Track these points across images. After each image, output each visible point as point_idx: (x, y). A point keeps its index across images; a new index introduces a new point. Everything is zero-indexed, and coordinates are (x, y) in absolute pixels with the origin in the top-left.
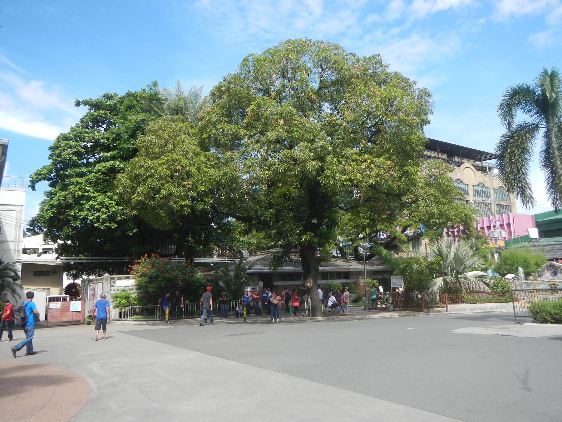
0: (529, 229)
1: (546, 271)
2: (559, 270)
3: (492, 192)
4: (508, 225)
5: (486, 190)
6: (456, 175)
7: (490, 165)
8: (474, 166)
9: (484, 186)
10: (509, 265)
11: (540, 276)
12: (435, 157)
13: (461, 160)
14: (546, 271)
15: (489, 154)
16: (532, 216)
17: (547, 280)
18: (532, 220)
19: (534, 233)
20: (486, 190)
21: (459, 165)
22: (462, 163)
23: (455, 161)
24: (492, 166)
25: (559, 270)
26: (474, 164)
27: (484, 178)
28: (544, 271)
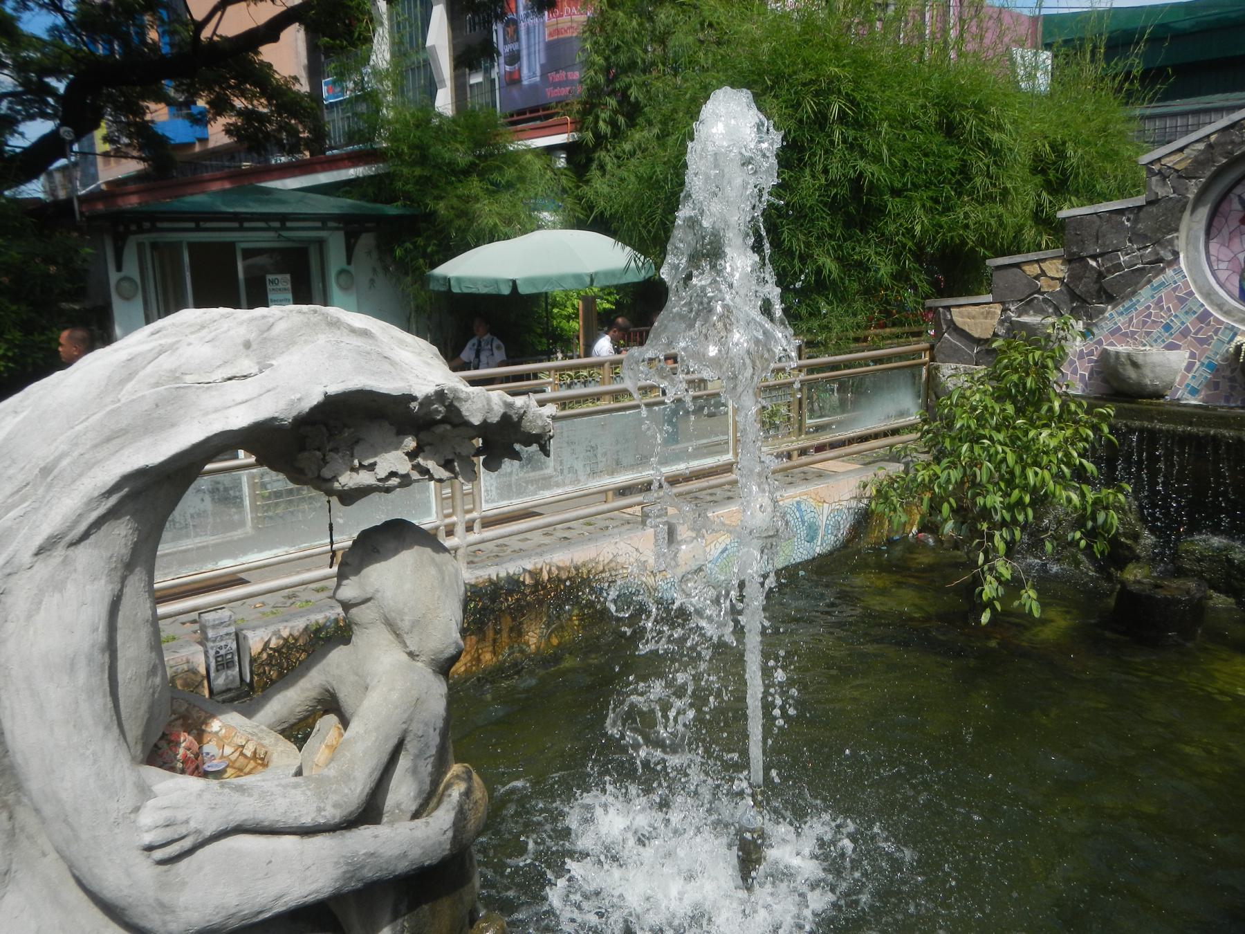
1: (1193, 224)
11: (1092, 293)
14: (1193, 224)
28: (1156, 225)
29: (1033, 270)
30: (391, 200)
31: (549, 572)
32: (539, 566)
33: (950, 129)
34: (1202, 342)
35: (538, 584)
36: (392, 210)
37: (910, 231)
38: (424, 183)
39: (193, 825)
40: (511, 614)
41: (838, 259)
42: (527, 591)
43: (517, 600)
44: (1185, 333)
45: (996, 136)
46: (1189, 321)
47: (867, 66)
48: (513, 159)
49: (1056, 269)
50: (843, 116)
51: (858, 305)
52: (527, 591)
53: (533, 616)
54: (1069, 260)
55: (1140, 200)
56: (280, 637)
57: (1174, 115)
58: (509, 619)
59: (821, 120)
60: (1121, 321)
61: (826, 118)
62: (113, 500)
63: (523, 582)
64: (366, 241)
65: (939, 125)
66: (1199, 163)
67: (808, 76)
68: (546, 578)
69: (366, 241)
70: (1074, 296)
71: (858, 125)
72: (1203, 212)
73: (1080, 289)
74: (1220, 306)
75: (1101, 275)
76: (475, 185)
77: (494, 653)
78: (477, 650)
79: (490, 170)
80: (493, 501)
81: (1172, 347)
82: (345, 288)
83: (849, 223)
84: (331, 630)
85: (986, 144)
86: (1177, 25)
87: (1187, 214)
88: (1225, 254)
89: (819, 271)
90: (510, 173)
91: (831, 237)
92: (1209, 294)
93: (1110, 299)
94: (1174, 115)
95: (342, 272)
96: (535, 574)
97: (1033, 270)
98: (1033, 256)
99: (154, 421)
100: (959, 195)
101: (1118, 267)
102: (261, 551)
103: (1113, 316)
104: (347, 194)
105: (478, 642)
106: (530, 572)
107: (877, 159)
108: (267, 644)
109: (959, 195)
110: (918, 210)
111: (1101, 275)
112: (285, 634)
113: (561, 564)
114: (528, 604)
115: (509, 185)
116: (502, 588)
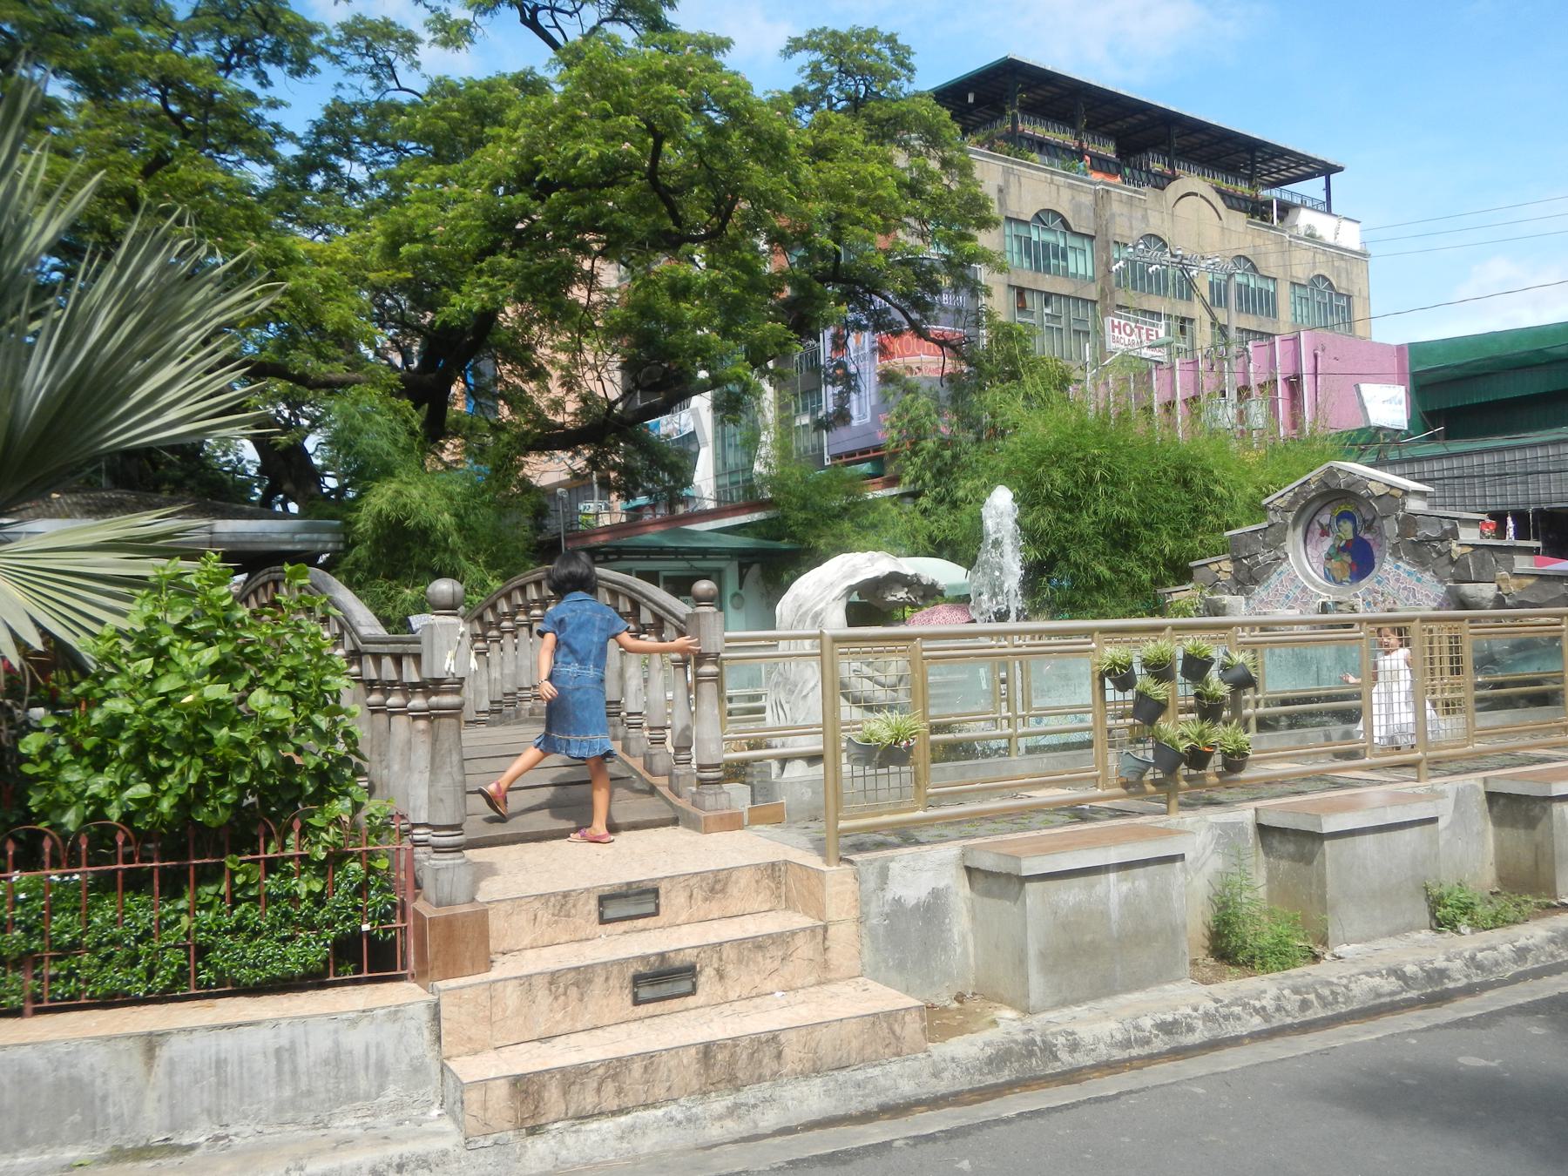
0: (1363, 387)
1: (1294, 539)
2: (1391, 528)
3: (1284, 296)
4: (1294, 384)
5: (1262, 284)
6: (1145, 218)
7: (1286, 197)
8: (1219, 191)
9: (1254, 268)
10: (1049, 500)
11: (1246, 580)
12: (1066, 149)
13: (1171, 166)
14: (1294, 539)
15: (1282, 153)
16: (1400, 348)
17: (1293, 614)
18: (1401, 364)
19: (1388, 406)
20: (1262, 284)
21: (1161, 182)
22: (1173, 178)
23: (1149, 171)
24: (1297, 200)
25: (1391, 528)
26: (1224, 186)
27: (1259, 241)
28: (1274, 538)
29: (1214, 567)
30: (779, 539)
33: (1186, 484)
34: (1306, 603)
36: (784, 544)
37: (1161, 551)
38: (809, 524)
41: (1111, 568)
44: (1296, 599)
45: (1218, 489)
46: (1297, 592)
47: (1118, 448)
48: (873, 505)
49: (1227, 566)
50: (1103, 478)
51: (1128, 600)
54: (1235, 560)
55: (1265, 525)
57: (1533, 446)
59: (1090, 480)
60: (1264, 594)
61: (1092, 478)
64: (755, 570)
65: (1177, 481)
66: (1292, 503)
67: (1080, 455)
69: (755, 570)
70: (1238, 582)
71: (1115, 485)
72: (1300, 530)
73: (1240, 577)
74: (1313, 583)
75: (1250, 569)
76: (847, 526)
79: (858, 515)
81: (1291, 608)
82: (737, 608)
83: (1115, 544)
85: (1209, 493)
86: (1555, 351)
87: (1290, 532)
88: (1315, 554)
89: (1098, 578)
90: (873, 517)
91: (1104, 554)
92: (1307, 577)
93: (1257, 582)
94: (1533, 446)
95: (735, 595)
97: (1214, 567)
98: (1214, 559)
99: (852, 575)
100: (1195, 528)
101: (1258, 563)
103: (1260, 591)
104: (745, 534)
107: (1129, 504)
109: (1195, 528)
110: (1164, 537)
111: (1250, 569)
115: (874, 526)
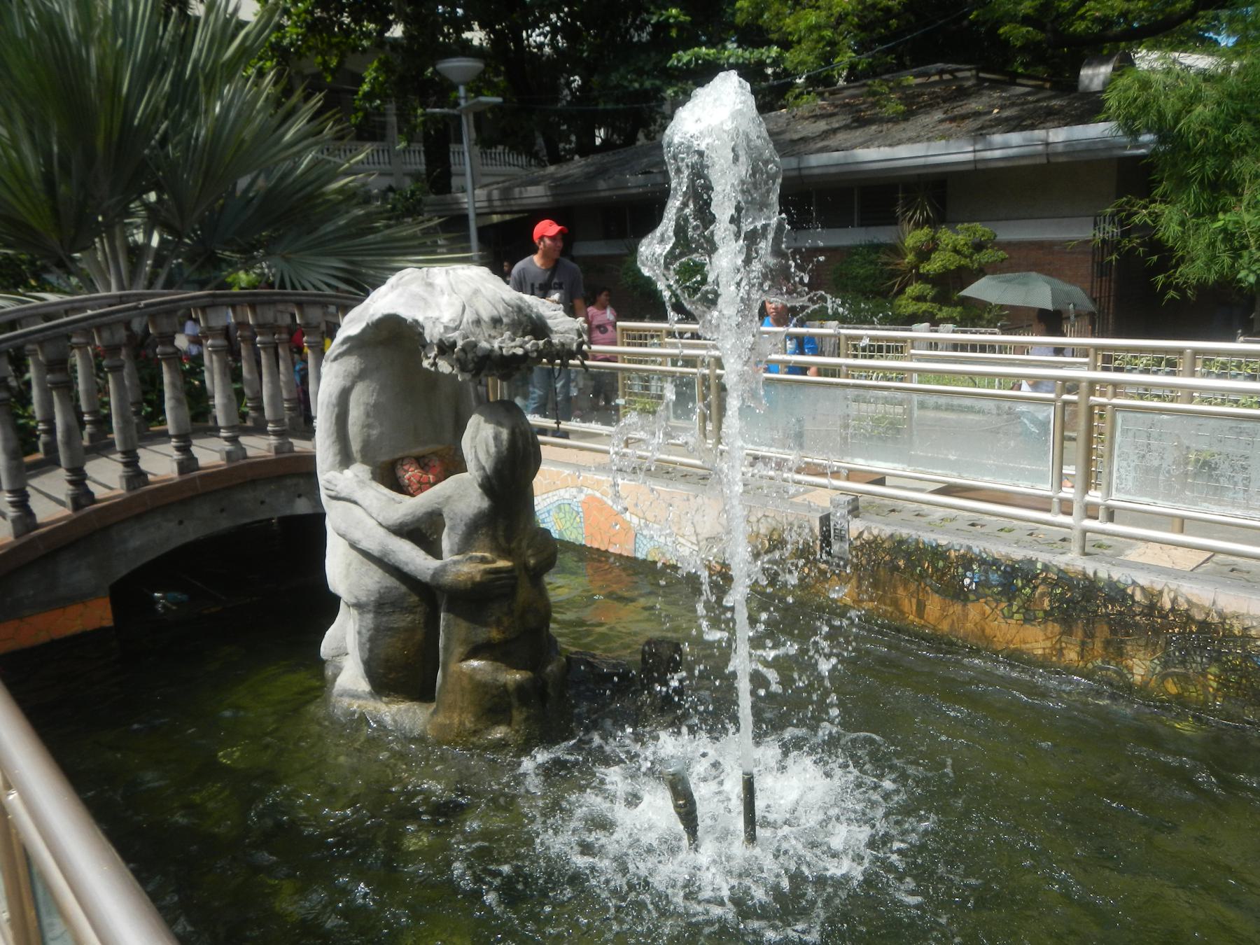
31: (1174, 601)
32: (1158, 588)
35: (1152, 607)
39: (337, 489)
40: (1108, 623)
42: (1137, 609)
43: (1120, 613)
52: (1137, 609)
53: (1142, 642)
56: (871, 533)
58: (1106, 628)
62: (345, 347)
63: (1132, 597)
68: (1168, 606)
77: (1082, 655)
78: (1059, 641)
80: (1128, 492)
84: (912, 547)
96: (1153, 597)
102: (886, 461)
105: (1062, 634)
106: (1142, 588)
108: (861, 533)
112: (875, 532)
113: (1195, 600)
114: (1136, 625)
116: (1101, 590)
